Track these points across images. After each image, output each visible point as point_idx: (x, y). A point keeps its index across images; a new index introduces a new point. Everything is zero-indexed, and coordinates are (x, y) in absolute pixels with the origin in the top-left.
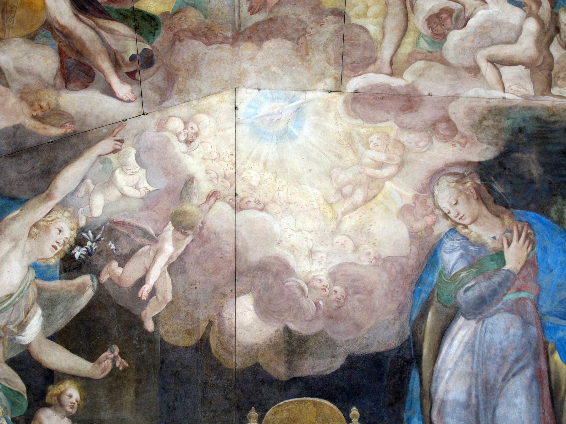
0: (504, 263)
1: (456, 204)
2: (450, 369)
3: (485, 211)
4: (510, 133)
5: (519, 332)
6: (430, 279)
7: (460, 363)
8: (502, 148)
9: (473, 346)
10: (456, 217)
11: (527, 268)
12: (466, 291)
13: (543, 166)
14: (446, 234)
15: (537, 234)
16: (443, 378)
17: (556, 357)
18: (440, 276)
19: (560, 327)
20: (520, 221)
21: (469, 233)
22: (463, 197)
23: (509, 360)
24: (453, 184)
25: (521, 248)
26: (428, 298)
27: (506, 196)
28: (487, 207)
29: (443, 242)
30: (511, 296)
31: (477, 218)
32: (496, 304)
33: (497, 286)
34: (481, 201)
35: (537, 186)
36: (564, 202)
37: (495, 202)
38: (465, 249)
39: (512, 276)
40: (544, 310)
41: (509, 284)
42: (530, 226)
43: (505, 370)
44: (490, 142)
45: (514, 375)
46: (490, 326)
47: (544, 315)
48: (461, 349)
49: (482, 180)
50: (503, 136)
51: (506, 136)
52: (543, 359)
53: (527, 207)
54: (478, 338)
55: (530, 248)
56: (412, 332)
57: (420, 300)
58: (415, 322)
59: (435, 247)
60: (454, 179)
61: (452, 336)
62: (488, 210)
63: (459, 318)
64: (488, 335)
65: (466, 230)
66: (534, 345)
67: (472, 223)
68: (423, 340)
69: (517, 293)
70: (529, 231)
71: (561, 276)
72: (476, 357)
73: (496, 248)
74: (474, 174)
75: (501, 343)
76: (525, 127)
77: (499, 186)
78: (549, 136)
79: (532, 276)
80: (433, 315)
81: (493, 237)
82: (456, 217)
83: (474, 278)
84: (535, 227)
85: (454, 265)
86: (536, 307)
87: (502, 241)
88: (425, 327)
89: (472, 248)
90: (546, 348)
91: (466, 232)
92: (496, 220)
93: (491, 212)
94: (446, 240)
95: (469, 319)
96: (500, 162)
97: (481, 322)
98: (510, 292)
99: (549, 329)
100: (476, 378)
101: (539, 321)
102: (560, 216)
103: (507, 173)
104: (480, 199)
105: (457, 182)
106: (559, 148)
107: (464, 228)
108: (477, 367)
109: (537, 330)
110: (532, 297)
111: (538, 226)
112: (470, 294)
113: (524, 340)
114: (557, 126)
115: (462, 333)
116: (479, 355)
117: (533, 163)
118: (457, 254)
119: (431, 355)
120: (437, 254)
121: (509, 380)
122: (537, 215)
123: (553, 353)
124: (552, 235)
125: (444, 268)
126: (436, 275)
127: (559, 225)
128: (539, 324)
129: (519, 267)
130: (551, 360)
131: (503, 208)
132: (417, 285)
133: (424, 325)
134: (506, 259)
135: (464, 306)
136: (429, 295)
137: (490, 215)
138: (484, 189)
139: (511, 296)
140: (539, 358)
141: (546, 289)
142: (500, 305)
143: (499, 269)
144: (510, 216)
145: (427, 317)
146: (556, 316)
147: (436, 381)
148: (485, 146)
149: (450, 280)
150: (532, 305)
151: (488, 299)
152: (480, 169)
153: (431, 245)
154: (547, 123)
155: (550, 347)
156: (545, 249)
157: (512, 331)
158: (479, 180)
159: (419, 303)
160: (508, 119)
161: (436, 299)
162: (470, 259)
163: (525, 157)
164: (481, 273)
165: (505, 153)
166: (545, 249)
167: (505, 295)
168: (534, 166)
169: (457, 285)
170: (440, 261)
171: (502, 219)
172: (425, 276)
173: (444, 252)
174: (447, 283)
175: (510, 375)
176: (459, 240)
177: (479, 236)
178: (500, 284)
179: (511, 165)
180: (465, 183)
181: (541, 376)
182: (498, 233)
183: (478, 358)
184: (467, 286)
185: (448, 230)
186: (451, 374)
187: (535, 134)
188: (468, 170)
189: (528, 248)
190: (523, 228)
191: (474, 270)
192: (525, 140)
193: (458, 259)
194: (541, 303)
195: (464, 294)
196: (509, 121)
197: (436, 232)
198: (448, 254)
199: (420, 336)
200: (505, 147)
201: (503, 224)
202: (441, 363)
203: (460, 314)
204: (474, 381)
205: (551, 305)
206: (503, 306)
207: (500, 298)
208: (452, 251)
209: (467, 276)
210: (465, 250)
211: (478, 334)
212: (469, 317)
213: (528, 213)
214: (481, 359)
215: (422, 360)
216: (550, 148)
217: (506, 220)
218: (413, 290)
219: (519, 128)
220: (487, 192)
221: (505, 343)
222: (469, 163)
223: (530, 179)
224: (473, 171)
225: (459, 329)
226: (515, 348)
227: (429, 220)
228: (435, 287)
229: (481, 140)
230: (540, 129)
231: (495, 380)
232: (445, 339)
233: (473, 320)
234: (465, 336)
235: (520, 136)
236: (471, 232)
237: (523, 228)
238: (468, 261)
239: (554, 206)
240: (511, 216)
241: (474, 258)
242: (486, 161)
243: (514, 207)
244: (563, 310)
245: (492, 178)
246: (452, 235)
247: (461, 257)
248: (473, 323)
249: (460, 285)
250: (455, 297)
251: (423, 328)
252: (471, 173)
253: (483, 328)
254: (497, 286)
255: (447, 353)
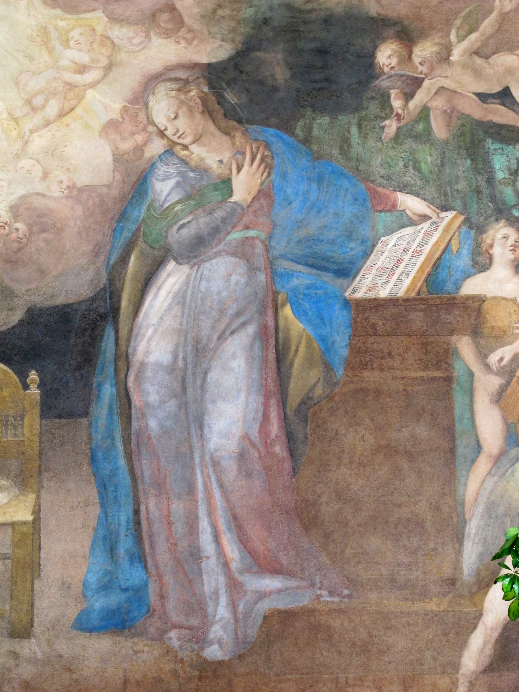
0: (231, 194)
1: (175, 118)
2: (153, 325)
3: (212, 128)
4: (252, 25)
5: (243, 280)
6: (136, 213)
7: (166, 318)
8: (240, 45)
9: (184, 297)
10: (174, 135)
11: (259, 200)
12: (179, 229)
13: (291, 68)
14: (160, 156)
15: (275, 156)
16: (144, 335)
17: (288, 310)
18: (148, 210)
19: (295, 273)
20: (255, 140)
21: (189, 156)
22: (184, 109)
23: (228, 315)
24: (173, 93)
25: (254, 174)
26: (132, 238)
27: (239, 107)
28: (214, 122)
29: (155, 167)
30: (236, 235)
31: (201, 136)
32: (216, 245)
33: (219, 223)
34: (207, 115)
35: (281, 94)
36: (314, 115)
37: (225, 115)
38: (183, 175)
39: (239, 210)
40: (276, 253)
41: (235, 220)
42: (268, 146)
43: (222, 326)
44: (225, 37)
45: (233, 333)
46: (206, 273)
47: (276, 258)
48: (169, 300)
49: (211, 86)
50: (242, 30)
51: (246, 30)
52: (270, 313)
53: (265, 123)
54: (190, 287)
55: (265, 175)
56: (109, 280)
57: (122, 240)
58: (113, 267)
59: (144, 174)
60: (175, 86)
61: (159, 285)
62: (216, 126)
63: (169, 262)
64: (204, 283)
65: (186, 152)
66: (260, 296)
67: (194, 142)
68: (122, 289)
69: (244, 232)
70: (266, 153)
71: (302, 210)
72: (186, 311)
73: (222, 174)
74: (201, 80)
75: (219, 293)
76: (271, 18)
77: (232, 95)
78: (302, 29)
79: (265, 210)
80: (137, 258)
81: (219, 161)
82: (174, 135)
83: (192, 212)
84: (274, 148)
85: (168, 195)
86: (267, 249)
87: (231, 165)
88: (126, 273)
89: (191, 174)
90: (275, 300)
91: (185, 154)
92: (225, 139)
93: (219, 128)
94: (159, 164)
95: (181, 264)
96: (235, 64)
97: (196, 267)
98: (235, 230)
99: (281, 275)
100: (186, 336)
101: (269, 266)
102: (307, 134)
103: (244, 78)
104: (206, 112)
105: (179, 90)
106: (313, 45)
107: (183, 150)
108: (187, 322)
109: (266, 278)
110: (263, 236)
111: (278, 146)
112: (185, 232)
113: (249, 289)
114: (313, 16)
115: (171, 280)
116: (190, 308)
117: (279, 64)
118: (172, 182)
119: (131, 308)
120: (146, 182)
121: (226, 339)
122: (278, 131)
123: (283, 305)
124: (295, 159)
125: (153, 200)
126: (144, 208)
127: (305, 144)
128: (269, 270)
129: (249, 199)
130: (280, 314)
131: (235, 123)
132: (119, 221)
133: (124, 272)
134: (234, 188)
135: (176, 247)
136: (133, 234)
137: (217, 133)
138: (212, 100)
139: (236, 235)
140: (266, 312)
141: (281, 226)
142: (221, 246)
143: (224, 201)
144: (243, 134)
145: (129, 261)
146: (292, 260)
147: (136, 339)
148: (219, 43)
149: (160, 214)
150: (261, 247)
151: (206, 239)
152: (209, 73)
153: (139, 170)
154: (300, 11)
155: (280, 298)
156: (284, 176)
157: (234, 278)
158: (207, 87)
159: (120, 244)
160: (250, 7)
161: (141, 239)
162: (188, 189)
163: (269, 56)
164: (200, 207)
165: (243, 51)
166: (284, 176)
167: (228, 233)
168: (279, 69)
169: (170, 221)
170: (150, 191)
171: (233, 138)
172: (129, 209)
173: (156, 179)
174: (157, 218)
175: (228, 332)
176: (176, 164)
177: (202, 159)
178: (224, 220)
179: (248, 68)
180: (189, 91)
181: (266, 334)
182: (226, 156)
183: (189, 311)
184: (182, 222)
185: (163, 151)
186: (155, 331)
187: (284, 26)
188: (194, 74)
189: (262, 175)
190: (258, 148)
191: (192, 202)
192: (270, 34)
193: (173, 189)
194: (273, 244)
195: (177, 233)
196: (251, 9)
197: (148, 154)
198: (161, 183)
199: (118, 285)
200: (243, 44)
201: (234, 144)
202: (143, 318)
203: (170, 257)
204: (182, 339)
205: (285, 246)
206: (226, 248)
207: (222, 238)
208: (166, 178)
209: (182, 210)
210: (183, 177)
211: (192, 282)
212: (181, 261)
213: (266, 129)
214: (192, 313)
215: (119, 314)
216: (302, 44)
217: (237, 139)
218: (113, 228)
219: (264, 19)
220: (216, 103)
221: (224, 294)
222: (195, 66)
223: (273, 86)
224: (200, 76)
225: (168, 276)
226: (237, 300)
227: (140, 138)
228: (141, 224)
229: (213, 36)
230: (291, 20)
231: (208, 338)
232: (150, 288)
233: (186, 265)
234: (174, 284)
235: (264, 29)
236: (192, 154)
237: (258, 148)
238: (185, 191)
239: (301, 121)
240: (245, 133)
241: (193, 187)
242: (217, 63)
243: (250, 122)
244: (300, 253)
245: (224, 84)
246: (167, 159)
247: (176, 187)
248: (185, 269)
249: (173, 221)
250: (166, 237)
251: (123, 274)
252: (198, 78)
253: (198, 275)
254: (219, 223)
255: (151, 305)
